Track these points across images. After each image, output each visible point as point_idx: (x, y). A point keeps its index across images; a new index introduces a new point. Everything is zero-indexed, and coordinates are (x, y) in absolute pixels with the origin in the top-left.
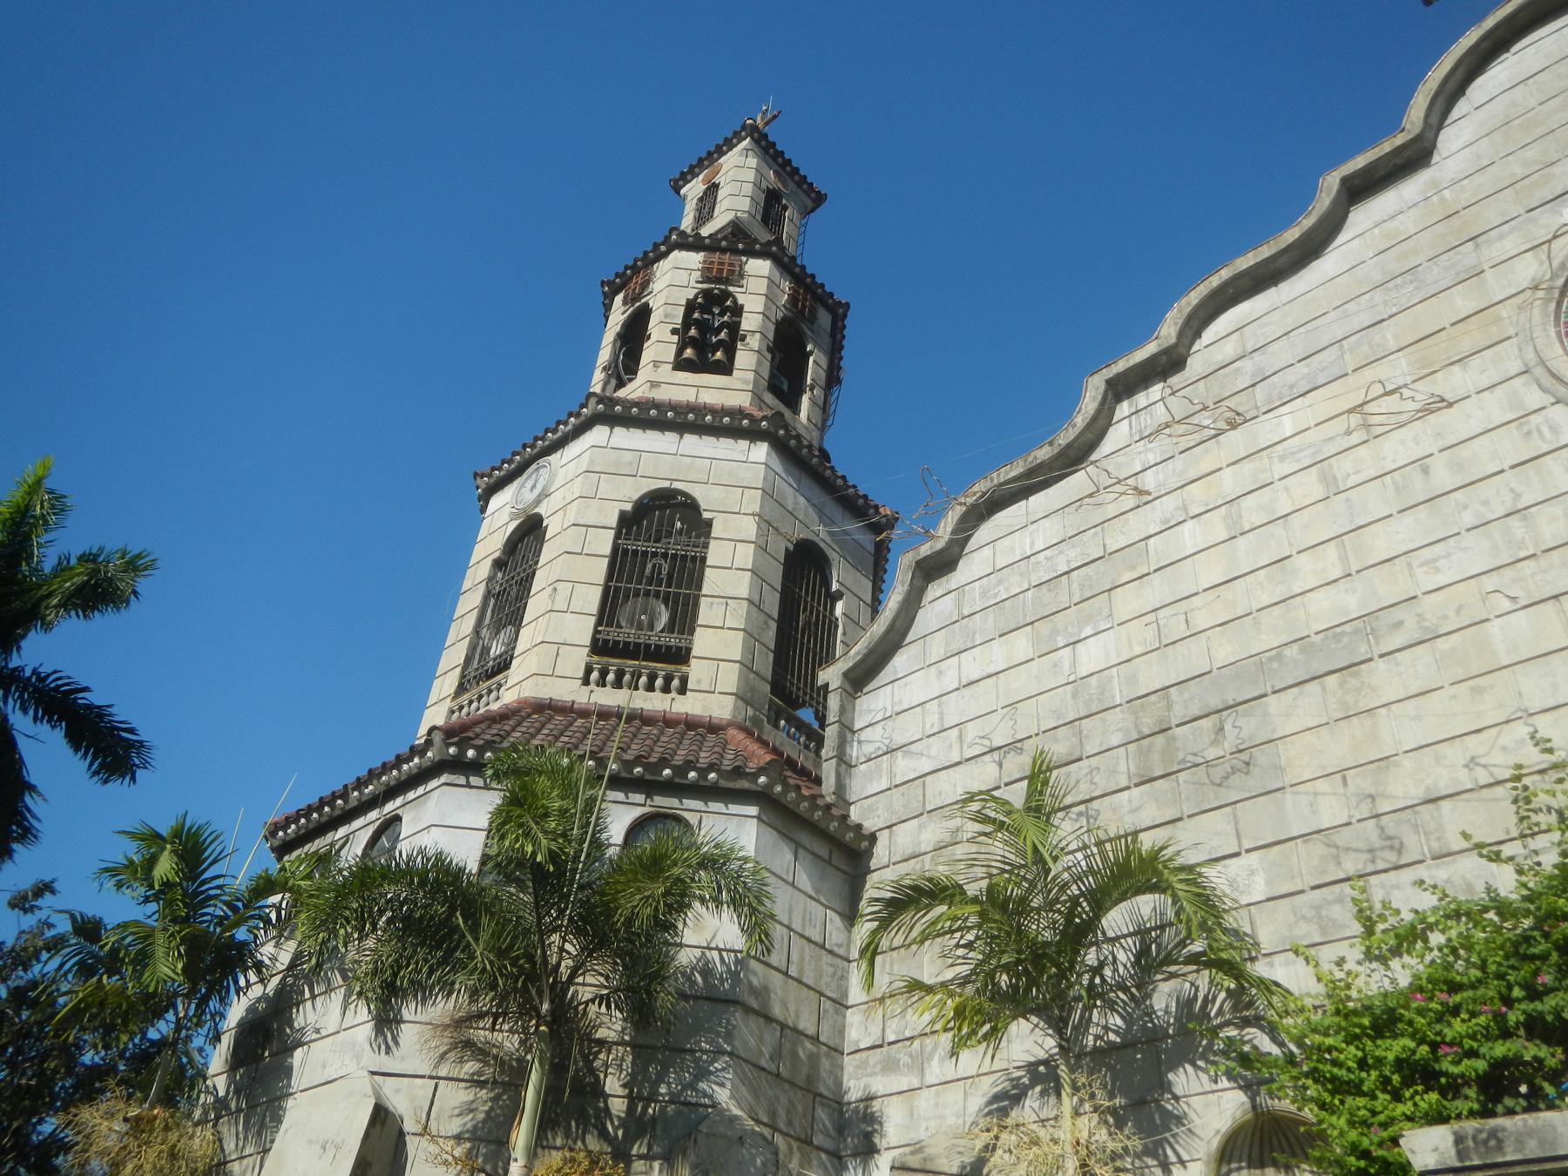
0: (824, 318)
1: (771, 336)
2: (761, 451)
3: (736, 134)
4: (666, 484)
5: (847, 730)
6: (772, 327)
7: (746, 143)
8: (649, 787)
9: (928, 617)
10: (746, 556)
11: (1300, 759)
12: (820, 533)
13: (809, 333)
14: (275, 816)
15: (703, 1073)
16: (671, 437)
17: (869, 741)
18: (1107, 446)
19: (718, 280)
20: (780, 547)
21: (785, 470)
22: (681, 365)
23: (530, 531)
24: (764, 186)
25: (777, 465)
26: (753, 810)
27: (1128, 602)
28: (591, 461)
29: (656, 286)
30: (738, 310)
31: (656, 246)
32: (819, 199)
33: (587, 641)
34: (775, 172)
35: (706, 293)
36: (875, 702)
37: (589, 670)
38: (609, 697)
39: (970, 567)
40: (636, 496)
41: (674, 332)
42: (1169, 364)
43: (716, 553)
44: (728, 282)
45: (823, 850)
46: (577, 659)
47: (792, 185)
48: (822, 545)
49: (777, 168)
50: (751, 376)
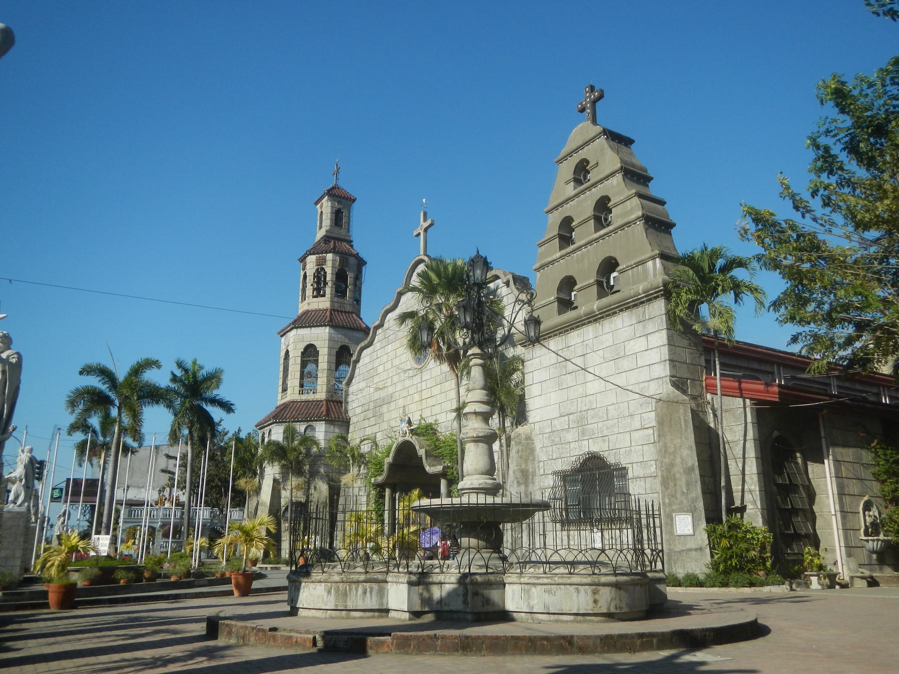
0: (352, 260)
1: (334, 280)
2: (327, 329)
3: (324, 195)
4: (309, 343)
5: (347, 395)
6: (334, 276)
7: (326, 197)
8: (308, 421)
9: (357, 371)
10: (326, 357)
11: (386, 417)
12: (346, 342)
13: (346, 269)
14: (256, 423)
15: (319, 467)
16: (309, 329)
17: (350, 399)
18: (375, 342)
19: (320, 265)
20: (334, 352)
21: (335, 331)
22: (314, 297)
23: (287, 352)
24: (334, 211)
25: (332, 331)
26: (324, 422)
27: (376, 379)
28: (294, 340)
29: (308, 267)
30: (325, 273)
31: (305, 254)
32: (354, 200)
33: (299, 385)
34: (339, 202)
35: (317, 270)
36: (352, 388)
37: (300, 391)
38: (304, 397)
39: (361, 361)
40: (304, 347)
41: (312, 285)
42: (381, 325)
43: (321, 359)
44: (323, 265)
45: (341, 424)
46: (297, 389)
47: (344, 201)
48: (347, 344)
49: (338, 199)
50: (329, 296)
